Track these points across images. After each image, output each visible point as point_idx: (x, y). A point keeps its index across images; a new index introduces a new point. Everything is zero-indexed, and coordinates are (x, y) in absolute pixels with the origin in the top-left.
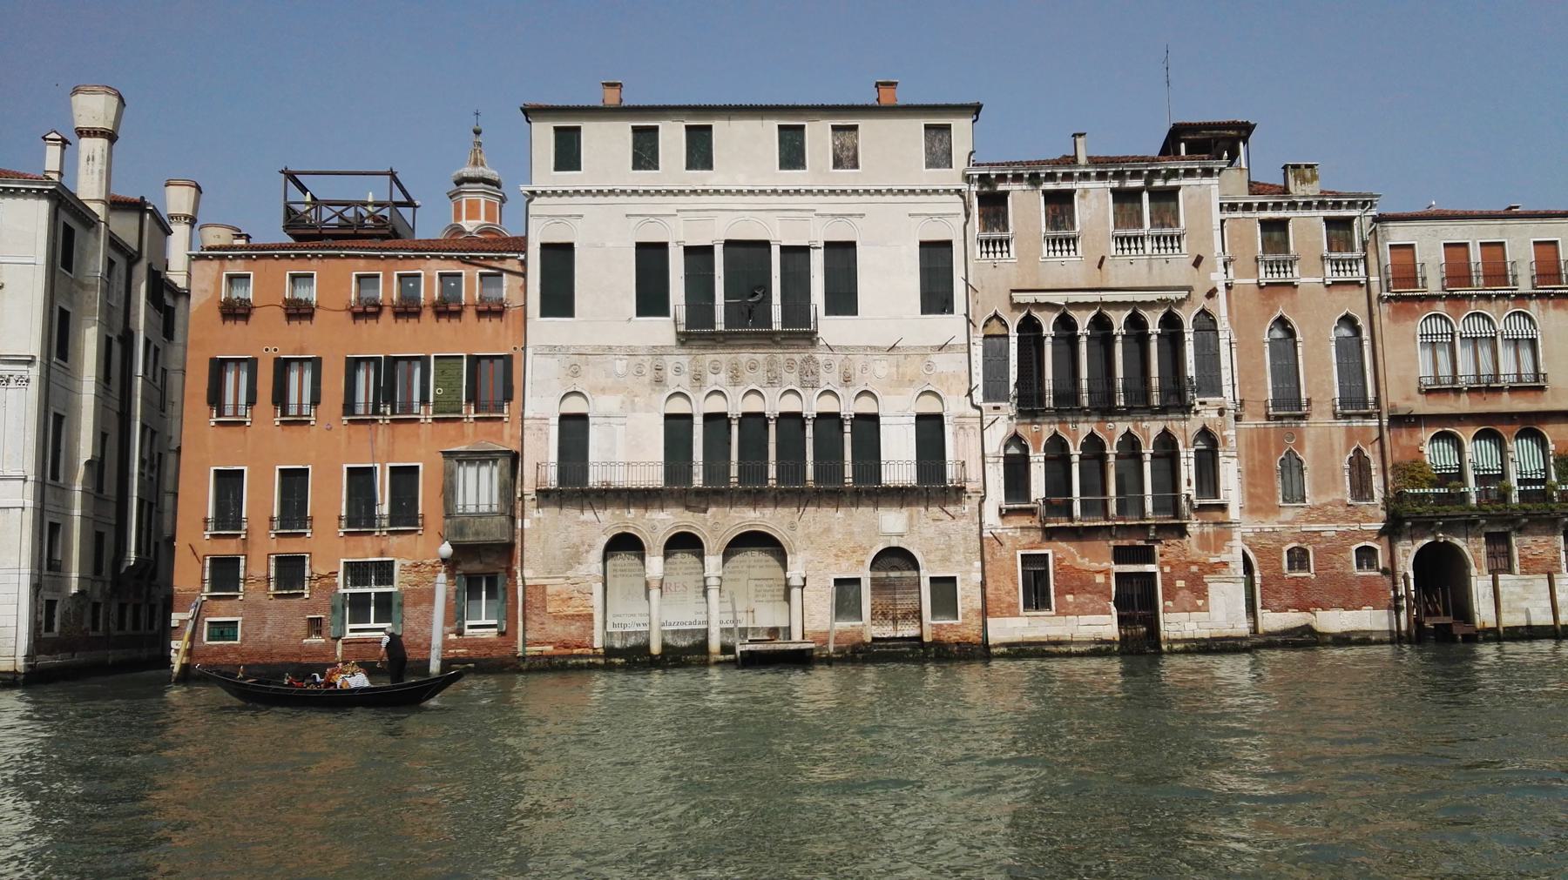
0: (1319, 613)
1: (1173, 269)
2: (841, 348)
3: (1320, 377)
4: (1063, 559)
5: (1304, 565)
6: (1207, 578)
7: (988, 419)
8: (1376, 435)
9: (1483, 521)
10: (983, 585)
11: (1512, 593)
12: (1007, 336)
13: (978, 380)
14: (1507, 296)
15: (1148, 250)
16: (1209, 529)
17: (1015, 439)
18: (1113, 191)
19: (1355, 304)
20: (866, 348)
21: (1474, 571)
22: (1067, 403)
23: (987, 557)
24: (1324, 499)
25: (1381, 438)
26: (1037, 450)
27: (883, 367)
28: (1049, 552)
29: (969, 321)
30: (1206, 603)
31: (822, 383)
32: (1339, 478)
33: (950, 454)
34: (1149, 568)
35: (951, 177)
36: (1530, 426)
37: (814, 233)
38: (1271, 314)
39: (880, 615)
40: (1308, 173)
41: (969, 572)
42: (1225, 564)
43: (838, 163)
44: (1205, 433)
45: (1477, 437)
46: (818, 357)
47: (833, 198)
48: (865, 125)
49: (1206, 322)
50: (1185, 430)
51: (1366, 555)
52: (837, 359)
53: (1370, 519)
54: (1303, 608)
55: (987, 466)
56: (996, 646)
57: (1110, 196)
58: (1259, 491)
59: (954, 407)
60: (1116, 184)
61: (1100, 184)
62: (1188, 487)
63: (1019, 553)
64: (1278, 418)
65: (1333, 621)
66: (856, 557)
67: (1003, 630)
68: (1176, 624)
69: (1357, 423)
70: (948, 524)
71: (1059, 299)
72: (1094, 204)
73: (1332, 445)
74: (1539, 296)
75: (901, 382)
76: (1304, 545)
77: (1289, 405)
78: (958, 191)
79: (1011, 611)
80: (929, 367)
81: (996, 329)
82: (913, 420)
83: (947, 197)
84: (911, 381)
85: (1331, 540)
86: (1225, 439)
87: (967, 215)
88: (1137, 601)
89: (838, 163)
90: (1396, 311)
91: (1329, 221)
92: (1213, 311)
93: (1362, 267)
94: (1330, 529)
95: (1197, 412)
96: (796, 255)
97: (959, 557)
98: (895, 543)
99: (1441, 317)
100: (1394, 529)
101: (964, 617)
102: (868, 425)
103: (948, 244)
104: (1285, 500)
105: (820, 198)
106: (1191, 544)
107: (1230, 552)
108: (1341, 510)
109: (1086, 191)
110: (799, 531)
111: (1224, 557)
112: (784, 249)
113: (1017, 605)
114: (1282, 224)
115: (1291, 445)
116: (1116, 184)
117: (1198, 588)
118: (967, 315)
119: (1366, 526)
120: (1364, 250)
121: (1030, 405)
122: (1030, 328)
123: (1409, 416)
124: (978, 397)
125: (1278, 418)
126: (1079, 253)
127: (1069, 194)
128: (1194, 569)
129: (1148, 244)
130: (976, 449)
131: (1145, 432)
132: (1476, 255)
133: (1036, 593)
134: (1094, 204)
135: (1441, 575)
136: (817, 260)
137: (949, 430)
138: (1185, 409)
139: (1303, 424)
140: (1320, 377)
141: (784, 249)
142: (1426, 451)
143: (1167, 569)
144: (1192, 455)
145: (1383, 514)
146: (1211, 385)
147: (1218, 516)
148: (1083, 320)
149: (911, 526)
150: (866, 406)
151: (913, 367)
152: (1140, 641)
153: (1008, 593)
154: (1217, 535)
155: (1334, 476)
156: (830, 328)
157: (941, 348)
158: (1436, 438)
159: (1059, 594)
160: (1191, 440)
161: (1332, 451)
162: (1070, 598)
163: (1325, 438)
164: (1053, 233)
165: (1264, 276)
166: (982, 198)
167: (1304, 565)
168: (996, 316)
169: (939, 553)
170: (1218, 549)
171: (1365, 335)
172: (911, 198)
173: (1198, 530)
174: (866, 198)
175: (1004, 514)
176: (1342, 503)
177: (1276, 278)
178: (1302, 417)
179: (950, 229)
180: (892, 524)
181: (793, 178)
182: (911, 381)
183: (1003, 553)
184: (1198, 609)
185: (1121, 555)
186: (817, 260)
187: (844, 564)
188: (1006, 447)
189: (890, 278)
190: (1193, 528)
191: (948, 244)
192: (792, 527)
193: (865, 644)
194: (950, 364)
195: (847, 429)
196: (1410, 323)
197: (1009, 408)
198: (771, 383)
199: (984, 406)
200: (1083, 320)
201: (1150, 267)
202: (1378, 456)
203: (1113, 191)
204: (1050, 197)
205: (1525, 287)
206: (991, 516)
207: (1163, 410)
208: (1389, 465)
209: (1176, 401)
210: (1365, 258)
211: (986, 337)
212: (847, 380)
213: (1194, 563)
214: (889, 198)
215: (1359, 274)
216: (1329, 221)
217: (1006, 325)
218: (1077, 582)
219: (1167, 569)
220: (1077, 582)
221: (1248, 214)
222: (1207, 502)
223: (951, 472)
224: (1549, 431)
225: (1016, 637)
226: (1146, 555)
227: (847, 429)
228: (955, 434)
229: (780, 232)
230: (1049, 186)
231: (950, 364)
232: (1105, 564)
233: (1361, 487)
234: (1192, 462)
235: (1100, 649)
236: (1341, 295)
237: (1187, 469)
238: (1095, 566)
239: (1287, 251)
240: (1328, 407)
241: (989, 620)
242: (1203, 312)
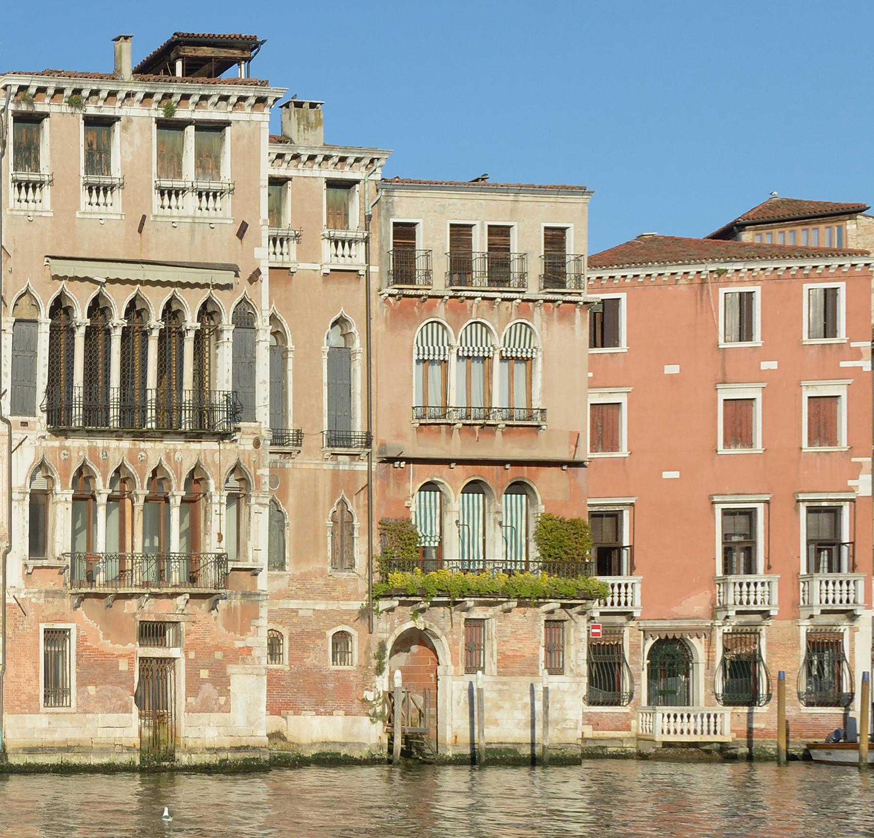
0: (292, 718)
19: (349, 301)
24: (305, 569)
25: (368, 486)
171: (358, 345)
176: (323, 572)
208: (375, 525)
210: (366, 240)
215: (356, 258)
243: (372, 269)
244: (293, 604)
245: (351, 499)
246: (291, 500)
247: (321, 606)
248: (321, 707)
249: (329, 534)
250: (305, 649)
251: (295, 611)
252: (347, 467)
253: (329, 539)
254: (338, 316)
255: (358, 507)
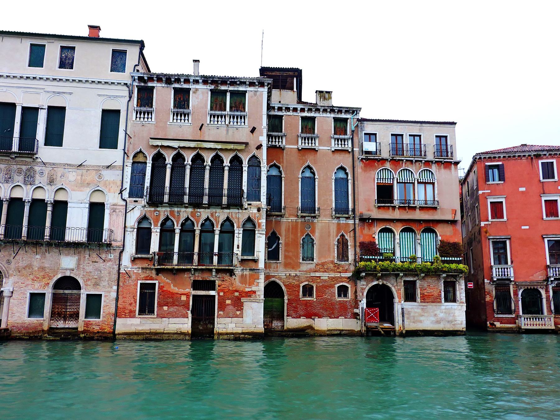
0: (317, 319)
1: (239, 132)
2: (50, 164)
3: (325, 198)
4: (163, 287)
5: (311, 295)
6: (243, 300)
7: (130, 207)
8: (352, 228)
9: (401, 274)
10: (117, 299)
11: (416, 312)
12: (146, 163)
13: (127, 185)
14: (421, 161)
15: (227, 123)
16: (247, 273)
17: (144, 218)
18: (211, 90)
19: (346, 161)
20: (65, 165)
21: (396, 300)
22: (176, 200)
23: (121, 284)
26: (156, 225)
27: (73, 176)
28: (156, 282)
29: (125, 153)
30: (242, 313)
31: (37, 182)
32: (332, 250)
33: (106, 225)
34: (212, 293)
35: (125, 77)
36: (429, 227)
37: (42, 100)
38: (303, 164)
39: (54, 315)
40: (327, 96)
41: (110, 292)
42: (254, 292)
43: (63, 65)
44: (249, 220)
45: (403, 231)
46: (37, 168)
47: (55, 83)
48: (78, 45)
49: (255, 162)
50: (238, 217)
51: (343, 291)
52: (46, 170)
53: (346, 271)
54: (309, 316)
55: (127, 233)
56: (119, 334)
57: (210, 93)
58: (291, 254)
59: (111, 199)
60: (213, 87)
61: (205, 87)
62: (237, 251)
63: (139, 282)
64: (302, 217)
65: (323, 324)
66: (45, 281)
67: (125, 325)
68: (224, 324)
69: (343, 221)
70: (101, 265)
71: (175, 144)
72: (201, 97)
73: (329, 232)
74: (436, 162)
75: (83, 184)
76: (311, 284)
77: (309, 208)
78: (126, 84)
79: (131, 314)
80: (100, 177)
81: (140, 159)
82: (87, 205)
83: (119, 87)
84: (88, 184)
85: (325, 281)
86: (260, 225)
87: (130, 97)
88: (203, 311)
89: (63, 65)
90: (366, 166)
91: (336, 119)
92: (259, 156)
93: (350, 142)
94: (325, 276)
95: (246, 209)
96: (30, 113)
97: (105, 283)
98: (68, 274)
99: (388, 170)
100: (357, 276)
101: (104, 317)
102: (61, 207)
103: (118, 112)
104: (303, 260)
105: (48, 83)
106: (236, 282)
107: (258, 285)
108: (332, 266)
109: (197, 90)
110: (13, 265)
111: (254, 288)
112: (24, 109)
113: (135, 312)
114: (313, 119)
115: (308, 231)
116: (213, 87)
117: (238, 305)
118: (124, 150)
119: (343, 275)
120: (352, 135)
121: (155, 201)
122: (158, 159)
123: (369, 219)
124: (126, 194)
125: (302, 217)
126: (190, 121)
127: (188, 91)
128: (237, 294)
129: (228, 119)
130: (121, 224)
131: (217, 219)
132: (407, 140)
133: (146, 307)
134: (200, 98)
135: (381, 300)
136: (42, 116)
137: (107, 212)
138: (240, 206)
139: (315, 221)
140: (325, 198)
141: (24, 109)
142: (377, 237)
143: (222, 294)
144: (241, 232)
145: (352, 268)
146: (255, 195)
147: (253, 265)
148: (189, 157)
149: (78, 265)
150: (61, 197)
151: (91, 176)
152: (202, 332)
153: (131, 304)
154: (251, 276)
155: (329, 248)
156: (46, 153)
157: (108, 167)
158: (382, 231)
159: (160, 305)
160: (241, 224)
161: (329, 236)
162: (165, 308)
163: (326, 228)
164: (176, 110)
165: (301, 144)
166: (140, 89)
167: (311, 295)
168: (141, 152)
169: (93, 281)
170: (250, 284)
171: (350, 177)
172: (100, 86)
173: (241, 273)
174: (74, 84)
175: (134, 260)
177: (307, 146)
178: (315, 217)
179: (120, 104)
180: (68, 263)
181: (36, 71)
182: (88, 184)
183: (131, 282)
184: (237, 316)
185: (197, 285)
186: (42, 116)
187: (37, 285)
188: (139, 222)
189: (83, 128)
190: (238, 272)
191: (118, 112)
192: (9, 262)
193: (43, 330)
194: (112, 176)
195: (49, 208)
196: (372, 172)
197: (143, 201)
198: (7, 182)
199: (128, 200)
200: (189, 157)
201: (227, 131)
202: (352, 238)
203: (211, 90)
204: (177, 91)
205: (430, 157)
206: (126, 261)
207: (228, 207)
209: (236, 202)
210: (352, 139)
211: (134, 163)
212: (51, 182)
213: (237, 291)
214: (87, 85)
215: (348, 146)
216: (336, 119)
217: (146, 157)
218: (170, 299)
219: (222, 294)
220: (170, 299)
221: (295, 114)
222: (245, 258)
223: (105, 236)
224: (439, 230)
225: (132, 330)
226: (211, 285)
227: (49, 208)
228: (110, 215)
229: (22, 99)
230: (177, 86)
231: (112, 176)
232: (187, 290)
233: (343, 255)
234: (241, 236)
235: (179, 336)
236: (338, 157)
237: (238, 240)
238: (181, 291)
239: (314, 133)
240: (328, 212)
241: (118, 320)
242: (254, 156)
243: (355, 149)
244: (317, 274)
245: (347, 234)
246: (317, 234)
247: (332, 275)
248: (332, 315)
249: (336, 247)
250: (324, 293)
251: (320, 277)
252: (344, 222)
253: (336, 250)
254: (340, 166)
255: (350, 237)
